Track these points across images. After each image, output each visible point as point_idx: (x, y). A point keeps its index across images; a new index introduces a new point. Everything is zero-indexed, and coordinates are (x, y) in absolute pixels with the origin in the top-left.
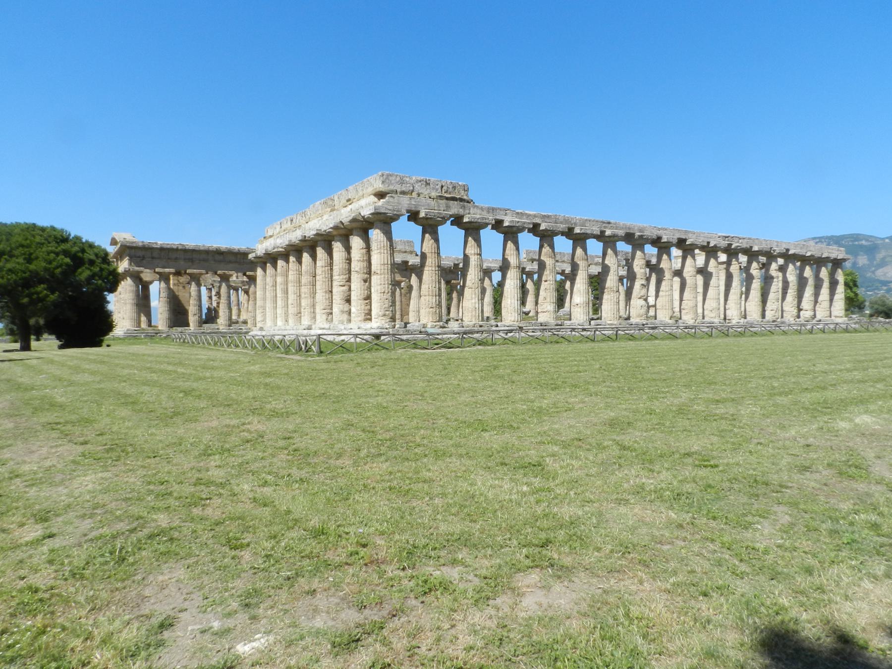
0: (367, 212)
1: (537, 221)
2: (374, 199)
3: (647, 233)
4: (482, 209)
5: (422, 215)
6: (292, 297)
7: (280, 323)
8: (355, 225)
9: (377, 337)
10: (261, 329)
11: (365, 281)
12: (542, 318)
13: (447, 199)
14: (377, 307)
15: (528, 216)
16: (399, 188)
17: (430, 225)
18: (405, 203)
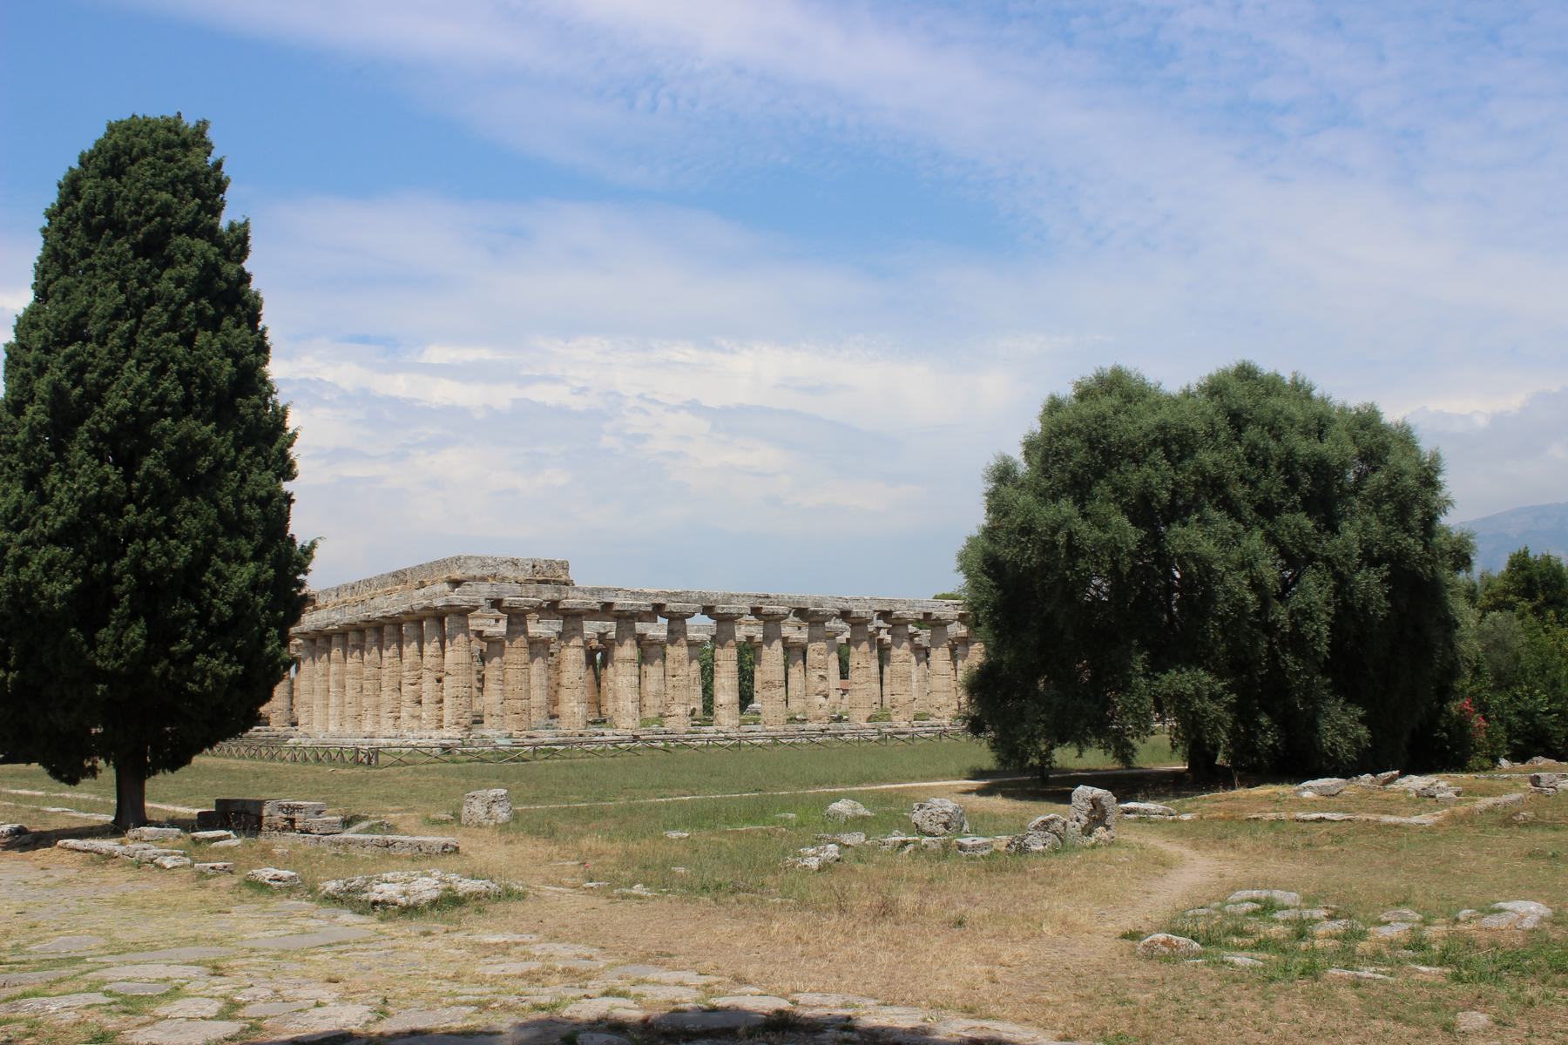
0: (439, 603)
1: (661, 601)
2: (446, 587)
3: (828, 608)
4: (584, 591)
5: (505, 604)
6: (350, 693)
7: (332, 728)
8: (425, 613)
9: (446, 749)
10: (307, 736)
11: (439, 680)
12: (670, 724)
13: (539, 582)
14: (448, 715)
15: (647, 595)
16: (478, 572)
17: (517, 615)
18: (485, 591)
